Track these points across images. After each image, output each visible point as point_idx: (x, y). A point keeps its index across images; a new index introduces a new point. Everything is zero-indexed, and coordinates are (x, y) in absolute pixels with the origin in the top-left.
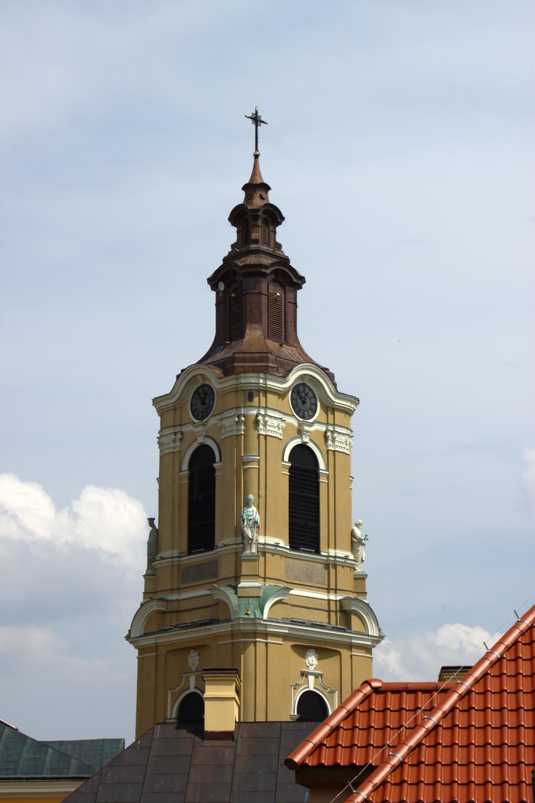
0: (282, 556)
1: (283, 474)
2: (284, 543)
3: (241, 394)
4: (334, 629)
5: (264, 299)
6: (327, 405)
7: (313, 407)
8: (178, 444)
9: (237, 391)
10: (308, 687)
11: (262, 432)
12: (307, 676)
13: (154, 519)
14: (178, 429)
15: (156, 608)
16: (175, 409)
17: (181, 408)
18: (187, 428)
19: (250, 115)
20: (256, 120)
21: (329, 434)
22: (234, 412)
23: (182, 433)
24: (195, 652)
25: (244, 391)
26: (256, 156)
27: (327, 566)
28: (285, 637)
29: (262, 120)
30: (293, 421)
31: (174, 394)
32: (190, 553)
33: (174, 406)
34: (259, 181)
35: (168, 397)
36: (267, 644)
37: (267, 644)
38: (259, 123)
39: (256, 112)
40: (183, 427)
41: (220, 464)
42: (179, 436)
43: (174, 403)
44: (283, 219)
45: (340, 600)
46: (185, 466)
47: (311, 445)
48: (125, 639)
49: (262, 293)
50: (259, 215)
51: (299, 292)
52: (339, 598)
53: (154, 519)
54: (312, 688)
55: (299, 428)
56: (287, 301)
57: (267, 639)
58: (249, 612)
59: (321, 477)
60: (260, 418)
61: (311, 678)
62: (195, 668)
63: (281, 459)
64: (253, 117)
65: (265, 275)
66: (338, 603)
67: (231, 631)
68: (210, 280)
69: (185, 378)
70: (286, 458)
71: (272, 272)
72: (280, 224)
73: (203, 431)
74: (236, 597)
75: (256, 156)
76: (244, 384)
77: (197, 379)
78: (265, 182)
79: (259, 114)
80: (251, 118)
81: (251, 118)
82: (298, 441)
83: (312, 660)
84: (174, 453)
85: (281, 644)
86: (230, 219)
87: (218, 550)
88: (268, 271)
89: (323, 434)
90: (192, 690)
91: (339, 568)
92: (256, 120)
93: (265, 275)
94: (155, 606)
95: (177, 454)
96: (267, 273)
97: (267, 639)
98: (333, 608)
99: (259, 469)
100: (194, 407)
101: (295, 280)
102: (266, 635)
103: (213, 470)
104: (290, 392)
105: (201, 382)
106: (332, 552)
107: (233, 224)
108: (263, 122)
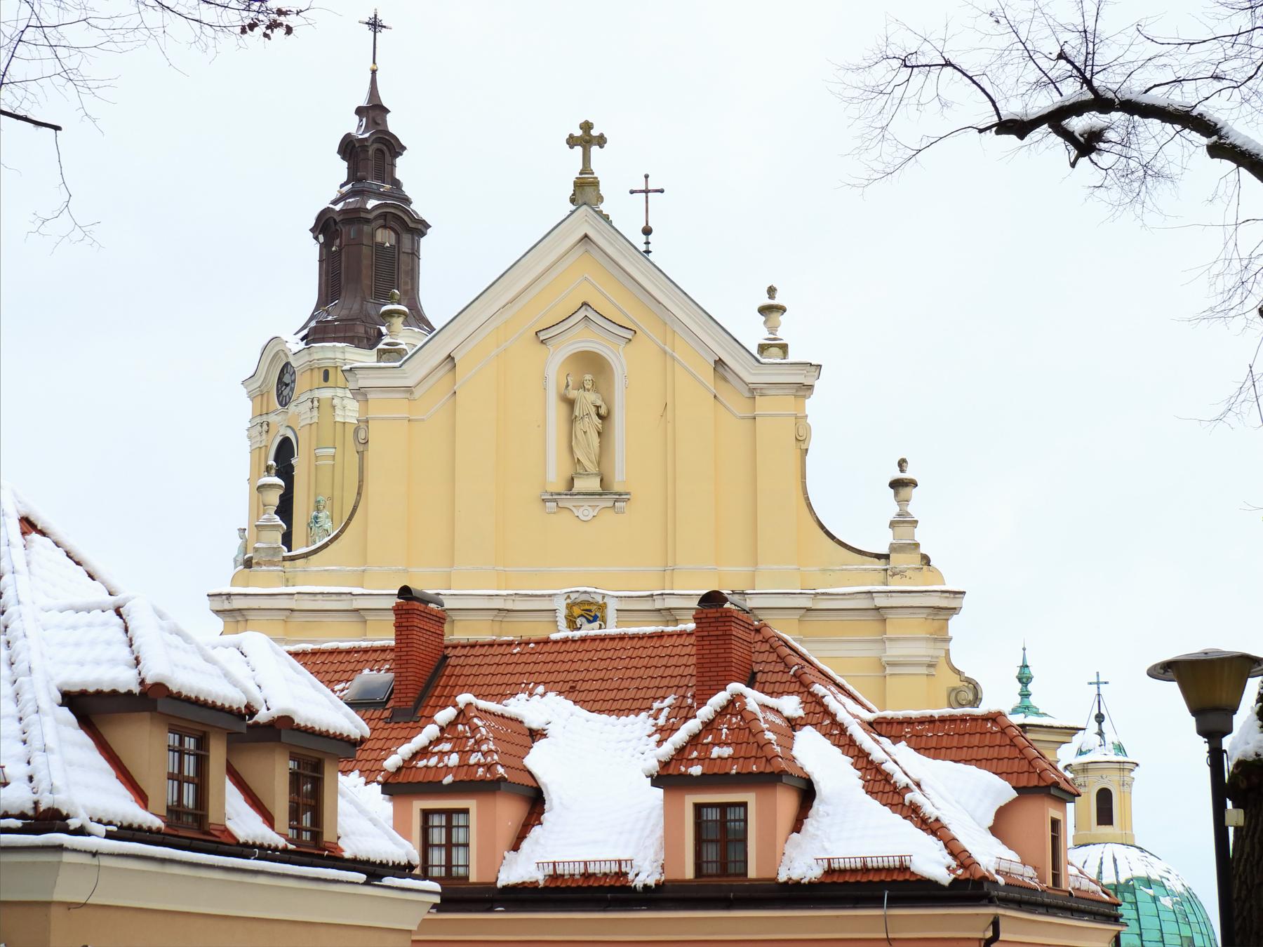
3: (316, 372)
9: (312, 369)
11: (338, 419)
14: (265, 418)
16: (262, 395)
17: (268, 392)
18: (272, 418)
19: (367, 20)
22: (308, 395)
23: (268, 425)
25: (319, 368)
26: (374, 72)
33: (261, 391)
39: (376, 15)
42: (265, 427)
43: (259, 387)
49: (363, 244)
50: (367, 146)
51: (423, 240)
53: (245, 529)
60: (336, 401)
64: (371, 22)
65: (367, 221)
69: (267, 358)
71: (377, 218)
72: (401, 155)
73: (285, 420)
75: (374, 72)
76: (318, 360)
77: (280, 356)
79: (379, 17)
81: (367, 23)
84: (260, 448)
86: (339, 152)
92: (375, 25)
93: (367, 221)
95: (264, 449)
108: (385, 27)
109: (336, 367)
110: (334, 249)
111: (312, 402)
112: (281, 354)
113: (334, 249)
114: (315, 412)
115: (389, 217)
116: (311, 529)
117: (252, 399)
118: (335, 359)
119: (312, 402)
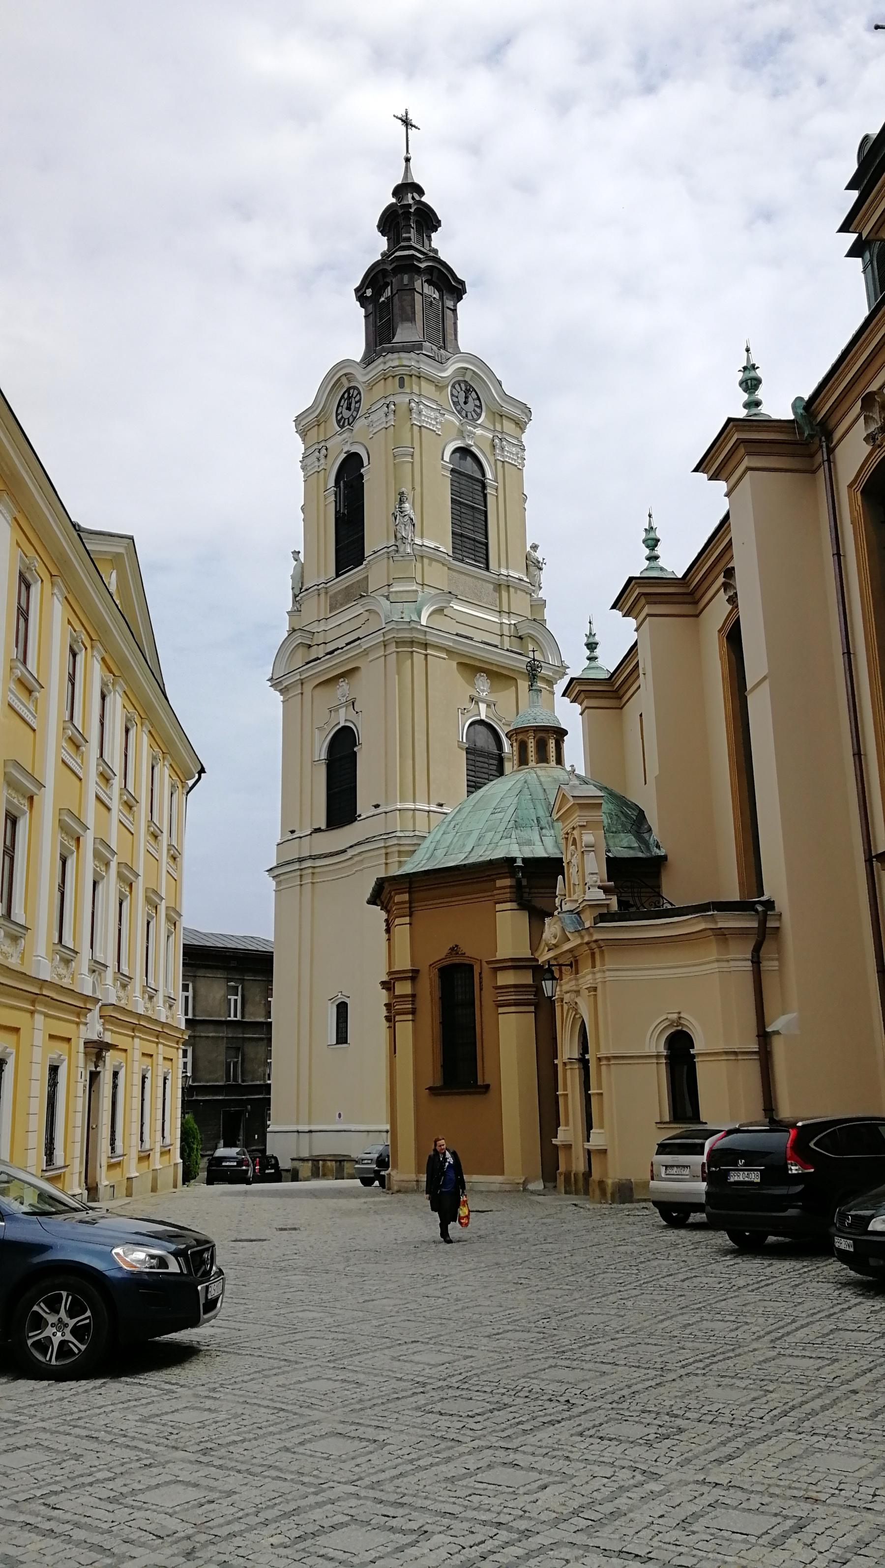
0: (443, 564)
1: (443, 475)
2: (446, 547)
4: (507, 650)
5: (418, 297)
6: (494, 411)
7: (478, 410)
8: (323, 461)
9: (385, 379)
10: (479, 715)
12: (477, 703)
13: (299, 552)
14: (323, 444)
15: (300, 641)
20: (406, 122)
21: (497, 441)
23: (327, 449)
24: (344, 681)
25: (393, 377)
26: (408, 160)
27: (498, 587)
28: (449, 652)
29: (413, 124)
30: (453, 419)
31: (318, 402)
32: (338, 576)
33: (318, 421)
34: (409, 181)
35: (311, 411)
36: (426, 655)
37: (426, 655)
38: (409, 127)
39: (407, 114)
40: (328, 442)
41: (369, 466)
42: (324, 451)
44: (439, 222)
45: (515, 624)
46: (332, 482)
47: (474, 449)
48: (270, 684)
52: (513, 622)
53: (299, 552)
54: (483, 717)
55: (461, 428)
56: (445, 306)
57: (426, 651)
58: (403, 615)
59: (488, 488)
61: (483, 707)
62: (345, 698)
63: (440, 457)
66: (513, 626)
67: (384, 641)
68: (355, 290)
70: (447, 458)
74: (388, 602)
75: (408, 160)
77: (342, 383)
78: (416, 181)
80: (400, 119)
82: (459, 444)
83: (483, 686)
85: (444, 659)
87: (368, 559)
88: (423, 265)
89: (489, 441)
90: (342, 724)
91: (512, 590)
92: (406, 122)
94: (298, 639)
96: (421, 268)
97: (426, 651)
98: (506, 632)
99: (412, 463)
100: (339, 417)
101: (453, 283)
102: (426, 646)
103: (361, 476)
104: (449, 388)
105: (346, 385)
106: (504, 571)
107: (383, 235)
108: (414, 126)
109: (411, 376)
110: (382, 299)
111: (388, 407)
112: (344, 380)
113: (382, 299)
114: (391, 416)
115: (435, 274)
116: (396, 519)
117: (303, 433)
118: (410, 367)
119: (388, 407)
